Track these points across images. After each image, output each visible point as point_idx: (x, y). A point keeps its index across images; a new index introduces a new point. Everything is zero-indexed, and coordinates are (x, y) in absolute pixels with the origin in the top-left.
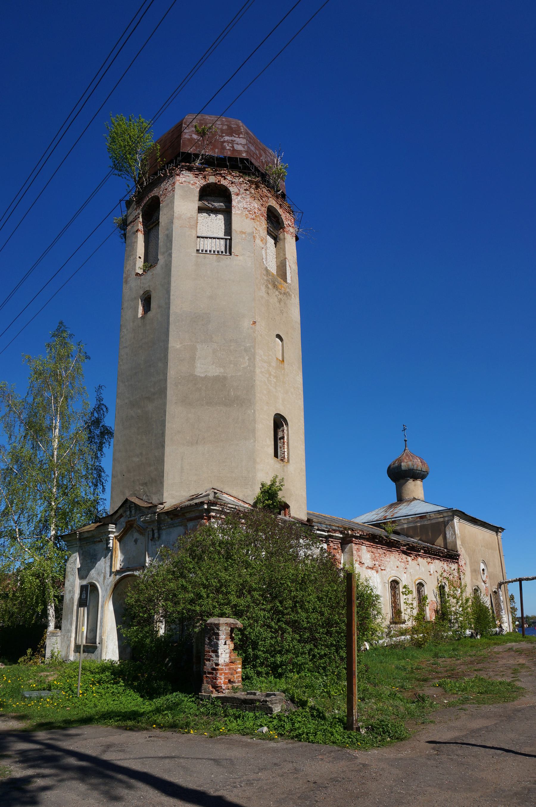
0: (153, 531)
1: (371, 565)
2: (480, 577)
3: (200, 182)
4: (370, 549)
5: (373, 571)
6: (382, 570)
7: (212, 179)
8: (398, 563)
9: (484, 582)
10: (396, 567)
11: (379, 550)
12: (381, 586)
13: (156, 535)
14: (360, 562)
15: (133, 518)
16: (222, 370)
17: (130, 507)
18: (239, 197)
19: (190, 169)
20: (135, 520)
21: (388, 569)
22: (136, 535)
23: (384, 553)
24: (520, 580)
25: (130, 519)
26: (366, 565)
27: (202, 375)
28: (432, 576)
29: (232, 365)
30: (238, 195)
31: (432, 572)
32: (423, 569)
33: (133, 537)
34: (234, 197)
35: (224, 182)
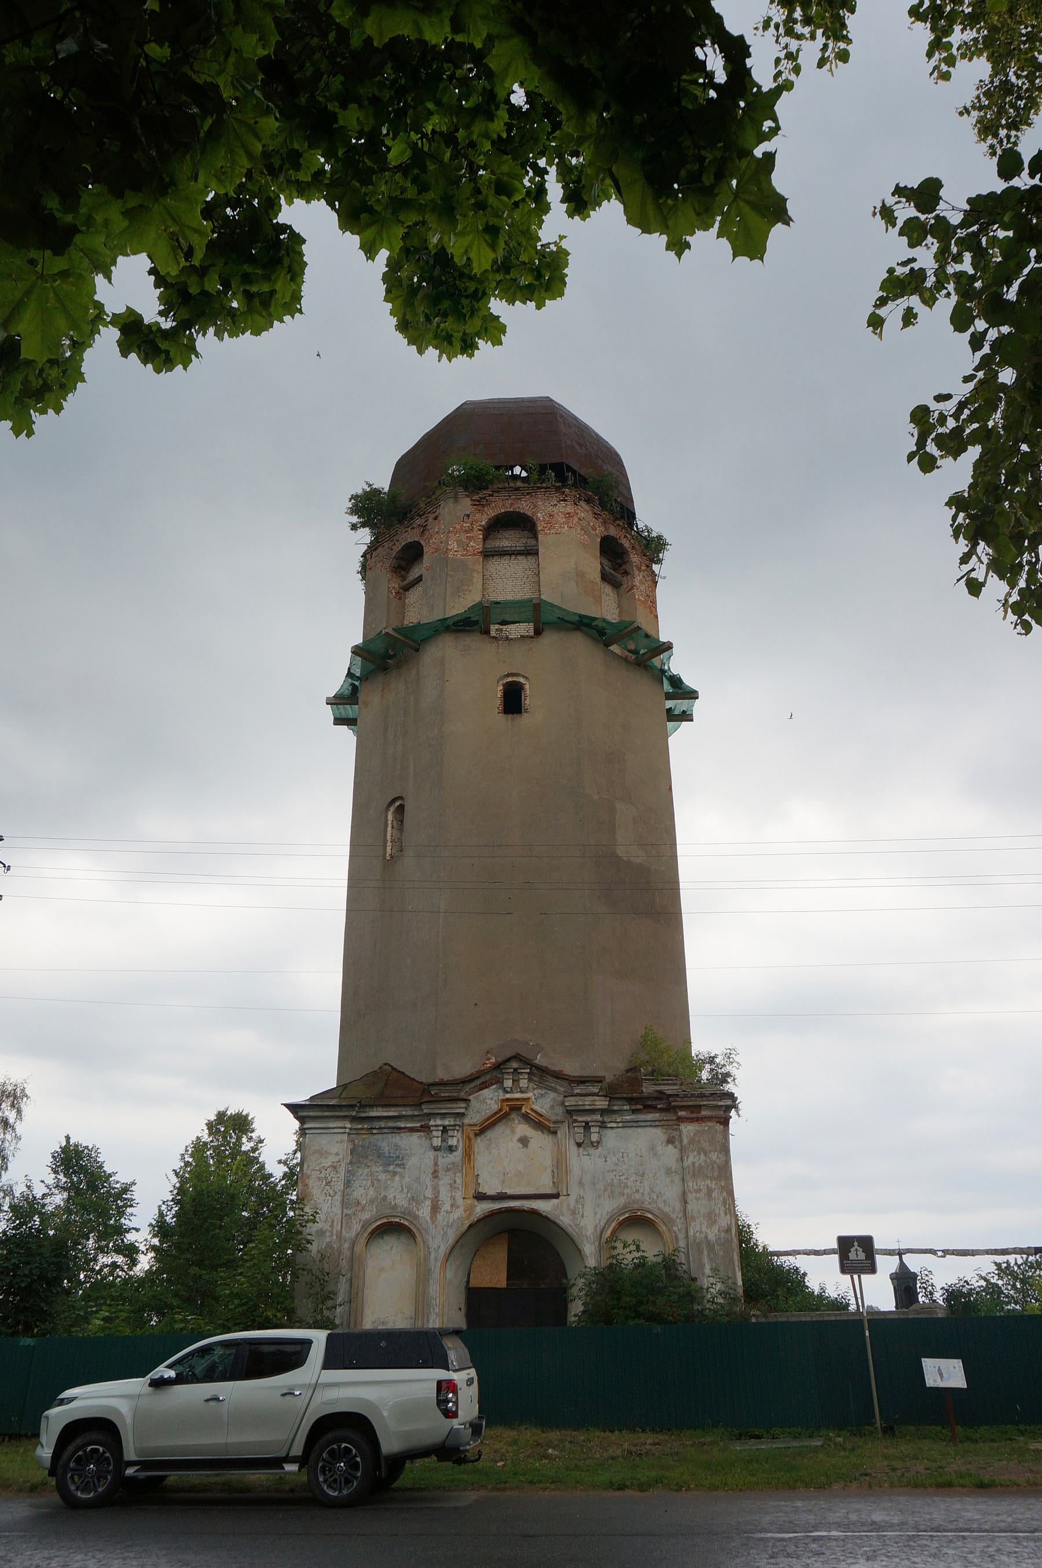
22: (523, 1129)
25: (508, 1096)
33: (513, 1131)
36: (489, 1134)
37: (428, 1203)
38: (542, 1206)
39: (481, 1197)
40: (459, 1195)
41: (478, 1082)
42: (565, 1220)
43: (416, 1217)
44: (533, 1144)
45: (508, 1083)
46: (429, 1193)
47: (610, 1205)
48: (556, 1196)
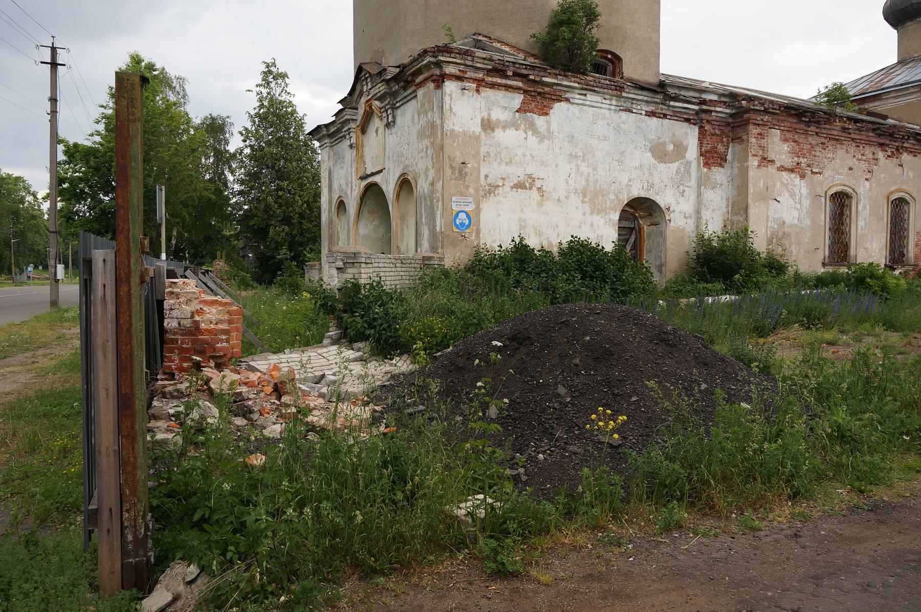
1: (789, 162)
4: (788, 135)
5: (793, 175)
6: (812, 172)
8: (853, 162)
10: (846, 169)
11: (810, 139)
12: (808, 201)
14: (765, 159)
21: (828, 173)
23: (822, 143)
26: (778, 164)
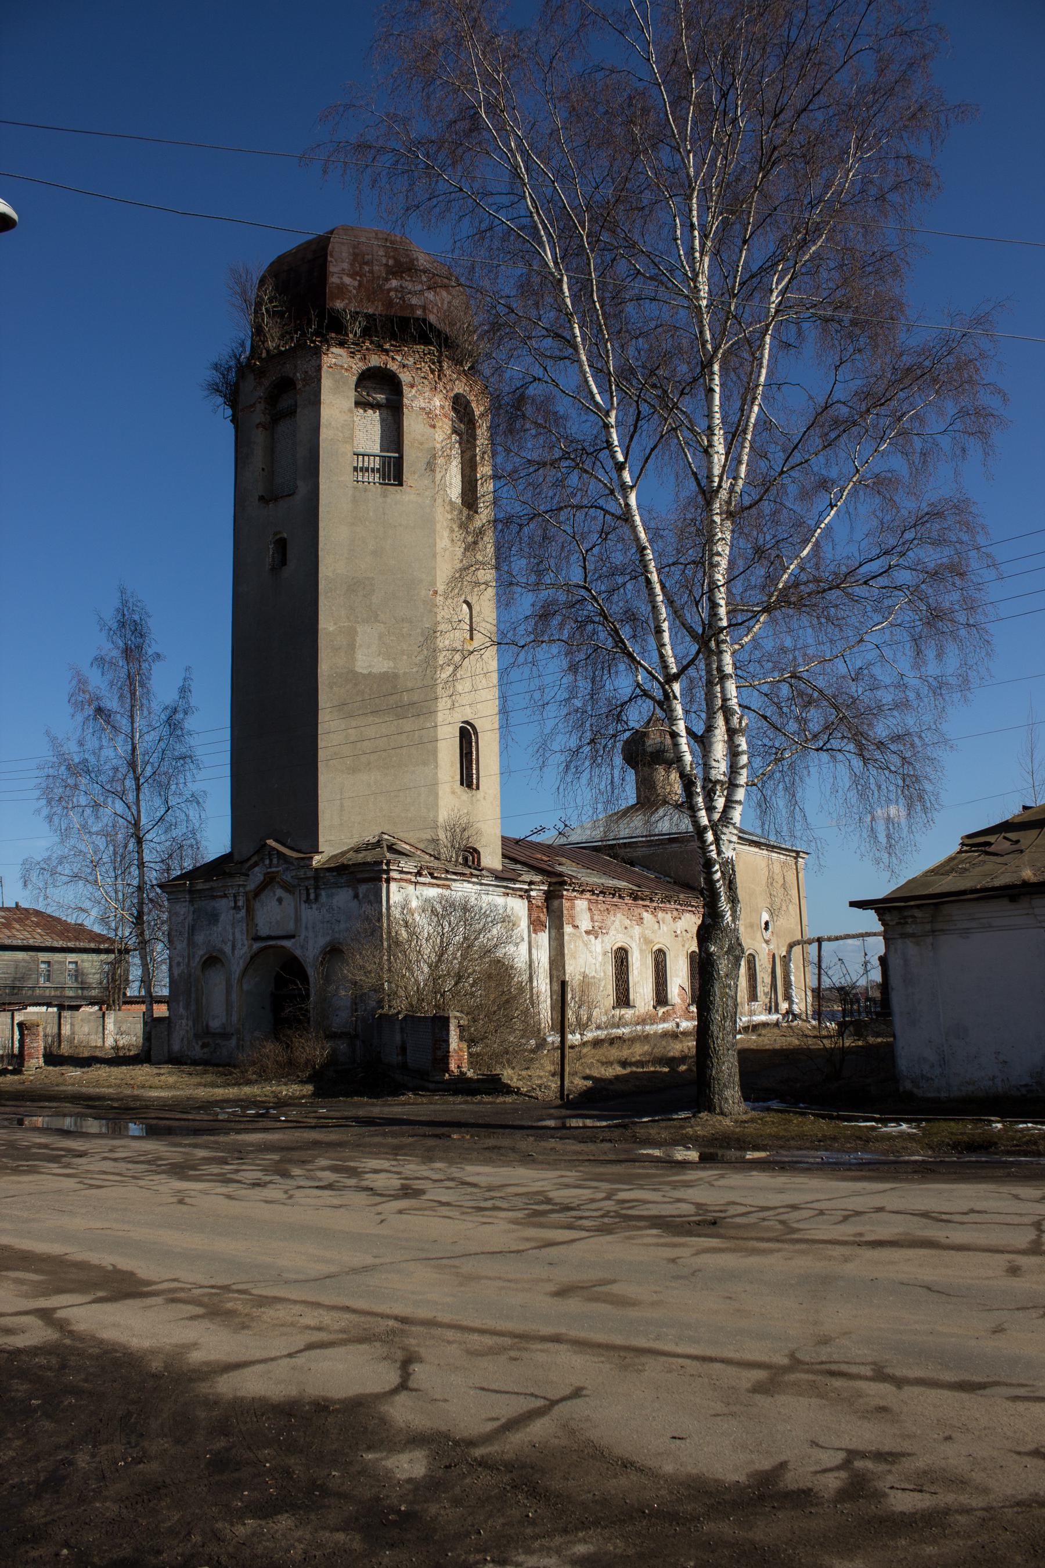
0: (307, 890)
2: (759, 934)
3: (357, 366)
7: (375, 360)
9: (767, 942)
13: (312, 896)
15: (273, 869)
16: (391, 664)
17: (270, 855)
18: (414, 391)
19: (342, 344)
20: (277, 872)
22: (280, 892)
24: (819, 940)
27: (365, 672)
28: (680, 939)
29: (405, 657)
30: (412, 386)
31: (679, 932)
32: (665, 929)
34: (406, 389)
35: (393, 366)
36: (263, 896)
37: (229, 944)
38: (287, 944)
39: (257, 938)
40: (245, 937)
41: (251, 862)
42: (298, 953)
43: (224, 953)
44: (285, 903)
45: (267, 862)
46: (231, 938)
47: (322, 941)
48: (293, 937)
